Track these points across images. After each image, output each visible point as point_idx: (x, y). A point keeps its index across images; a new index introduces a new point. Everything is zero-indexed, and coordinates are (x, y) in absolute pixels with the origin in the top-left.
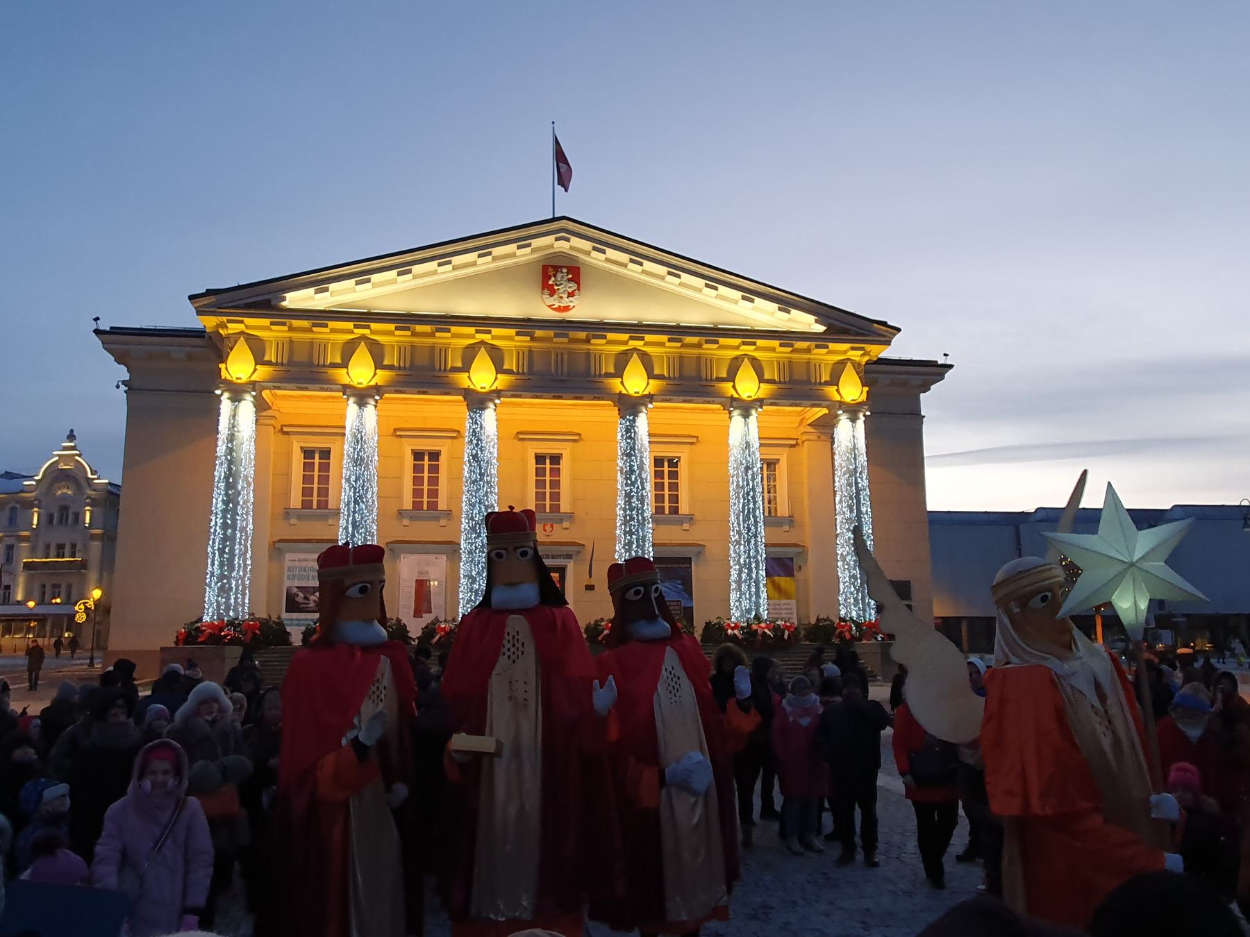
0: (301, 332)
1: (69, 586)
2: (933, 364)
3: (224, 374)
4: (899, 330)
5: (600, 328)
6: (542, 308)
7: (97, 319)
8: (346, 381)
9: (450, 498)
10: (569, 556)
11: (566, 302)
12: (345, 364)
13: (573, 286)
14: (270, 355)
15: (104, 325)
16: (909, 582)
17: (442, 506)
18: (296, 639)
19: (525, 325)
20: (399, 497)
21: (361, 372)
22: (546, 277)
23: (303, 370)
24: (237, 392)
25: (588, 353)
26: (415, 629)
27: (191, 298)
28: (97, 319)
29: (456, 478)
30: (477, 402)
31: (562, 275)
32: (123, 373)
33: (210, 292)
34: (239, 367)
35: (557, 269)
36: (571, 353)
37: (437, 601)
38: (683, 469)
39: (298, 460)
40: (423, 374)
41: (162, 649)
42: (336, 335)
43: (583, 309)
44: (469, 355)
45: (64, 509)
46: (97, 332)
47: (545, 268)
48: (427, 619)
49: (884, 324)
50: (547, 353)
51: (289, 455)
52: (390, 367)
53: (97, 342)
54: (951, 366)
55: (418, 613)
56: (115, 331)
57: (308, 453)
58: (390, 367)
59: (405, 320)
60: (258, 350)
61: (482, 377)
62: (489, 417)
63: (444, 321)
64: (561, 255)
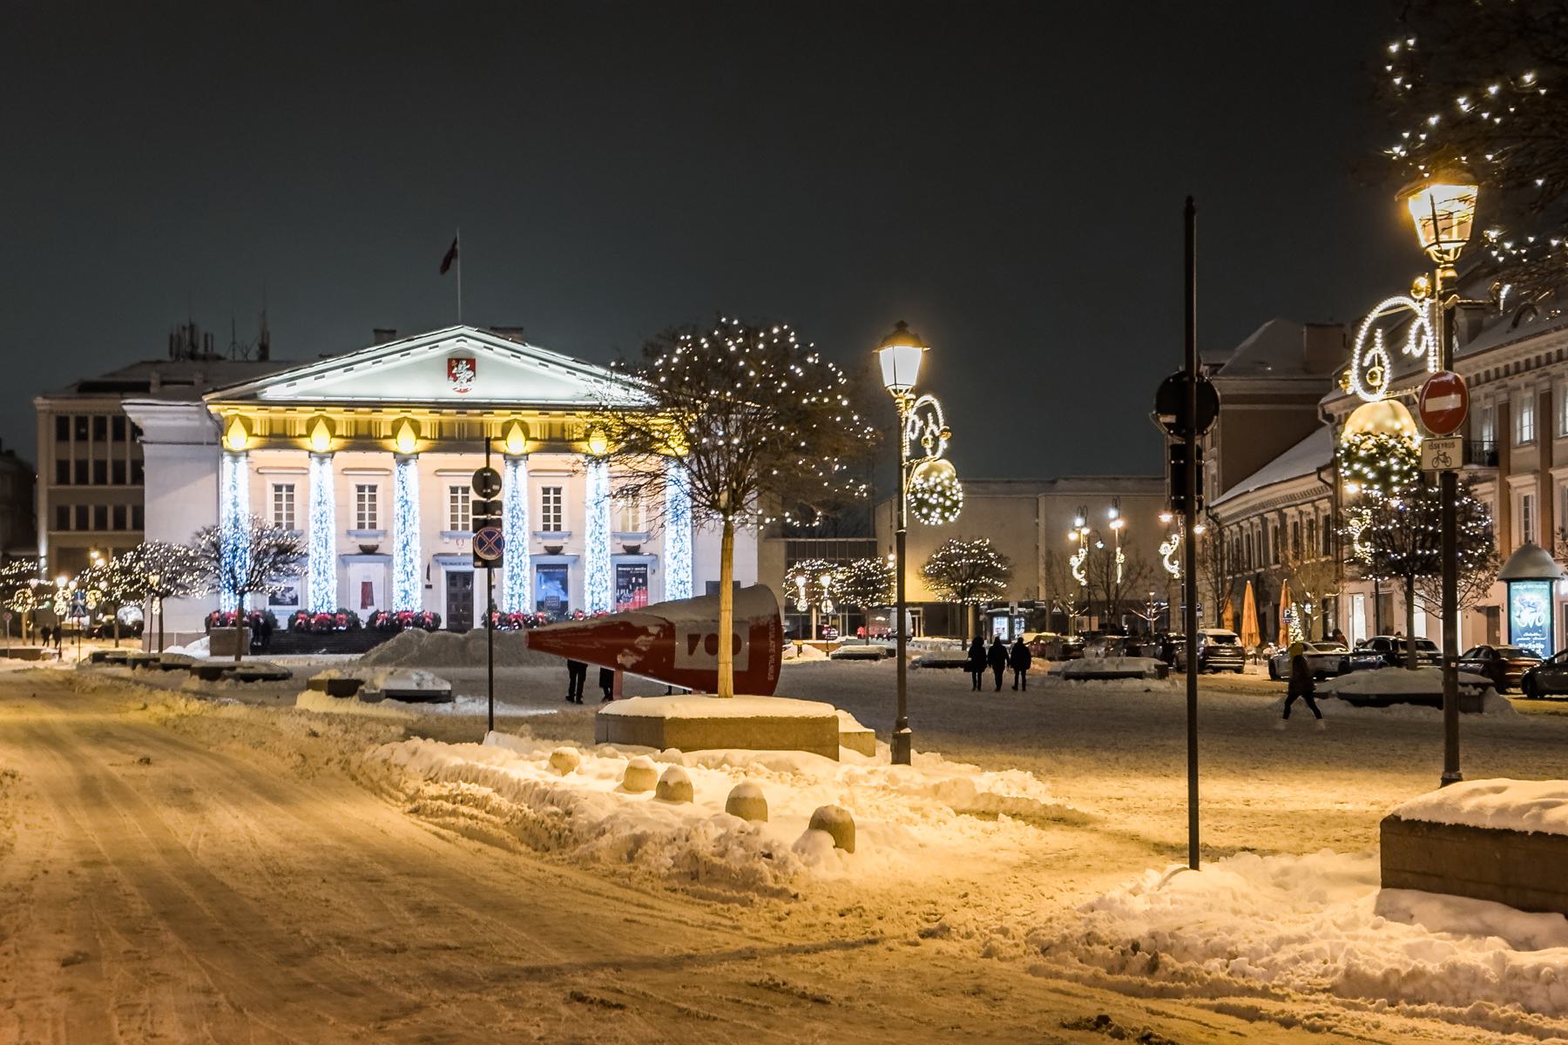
0: (278, 414)
3: (226, 444)
5: (489, 407)
6: (447, 390)
8: (310, 447)
9: (386, 520)
11: (465, 385)
12: (308, 435)
13: (471, 373)
14: (257, 430)
17: (380, 527)
18: (283, 624)
19: (437, 406)
20: (348, 520)
21: (321, 440)
22: (450, 368)
23: (279, 439)
24: (235, 456)
25: (482, 424)
26: (364, 616)
29: (389, 506)
30: (403, 460)
31: (463, 365)
34: (236, 438)
35: (458, 361)
36: (470, 424)
37: (378, 595)
38: (564, 495)
39: (271, 493)
40: (364, 440)
42: (302, 416)
43: (479, 389)
44: (396, 427)
47: (450, 360)
48: (371, 610)
50: (452, 424)
51: (264, 490)
52: (341, 437)
55: (364, 606)
57: (278, 488)
58: (341, 437)
59: (350, 405)
60: (248, 425)
61: (406, 442)
62: (412, 469)
63: (377, 405)
64: (461, 350)
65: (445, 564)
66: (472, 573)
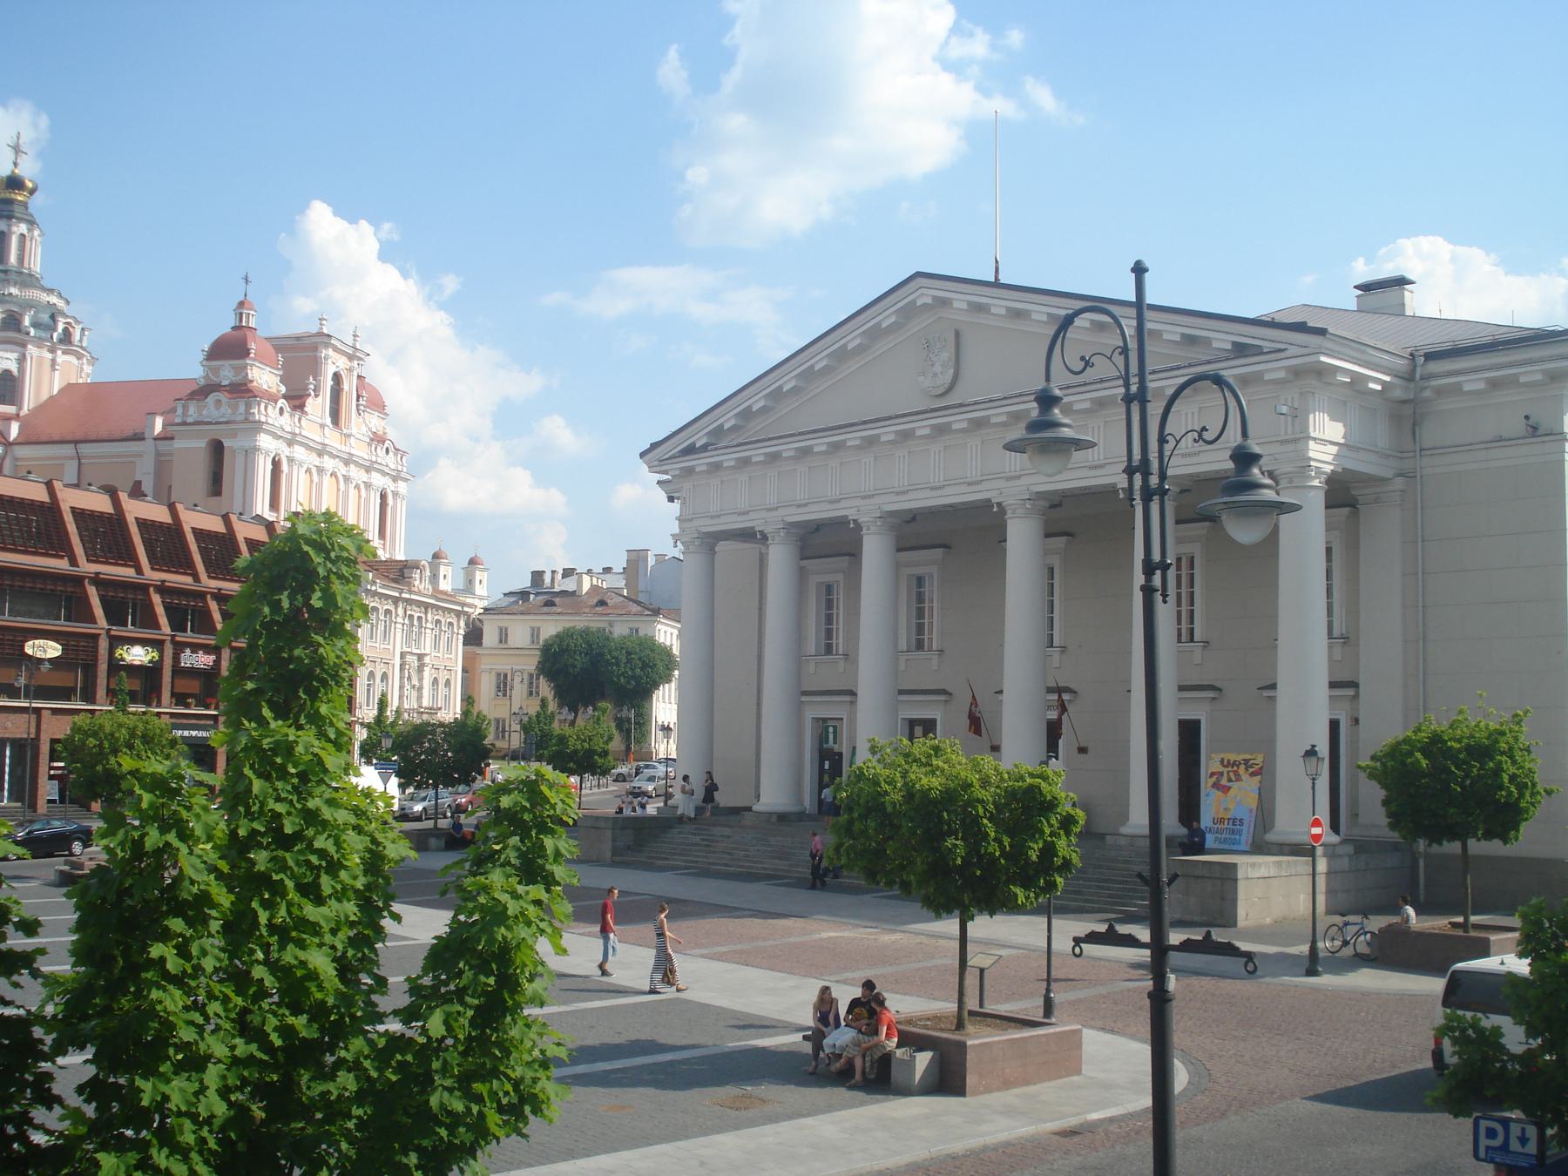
27: (642, 455)
33: (654, 446)
49: (1301, 327)
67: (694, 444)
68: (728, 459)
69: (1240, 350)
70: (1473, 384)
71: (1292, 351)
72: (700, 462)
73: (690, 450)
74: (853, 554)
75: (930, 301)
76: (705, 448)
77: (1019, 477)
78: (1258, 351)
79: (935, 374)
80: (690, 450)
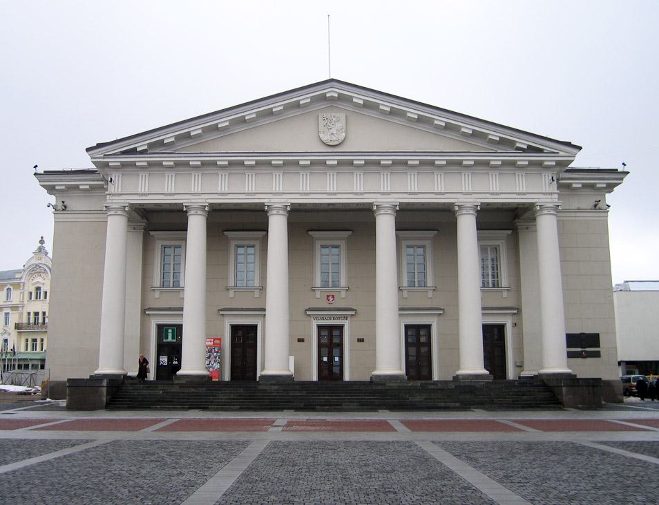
1: (42, 340)
2: (615, 171)
4: (580, 148)
7: (36, 166)
10: (345, 317)
15: (40, 170)
16: (598, 334)
27: (88, 150)
28: (36, 166)
32: (52, 199)
33: (99, 146)
41: (69, 380)
45: (38, 289)
46: (35, 174)
49: (569, 144)
53: (35, 179)
54: (629, 173)
56: (47, 173)
65: (316, 317)
66: (341, 328)
67: (136, 148)
68: (168, 161)
69: (531, 149)
70: (577, 184)
71: (561, 153)
72: (141, 161)
73: (133, 151)
74: (264, 228)
75: (336, 95)
76: (142, 152)
77: (389, 193)
78: (541, 151)
79: (333, 134)
80: (133, 151)
